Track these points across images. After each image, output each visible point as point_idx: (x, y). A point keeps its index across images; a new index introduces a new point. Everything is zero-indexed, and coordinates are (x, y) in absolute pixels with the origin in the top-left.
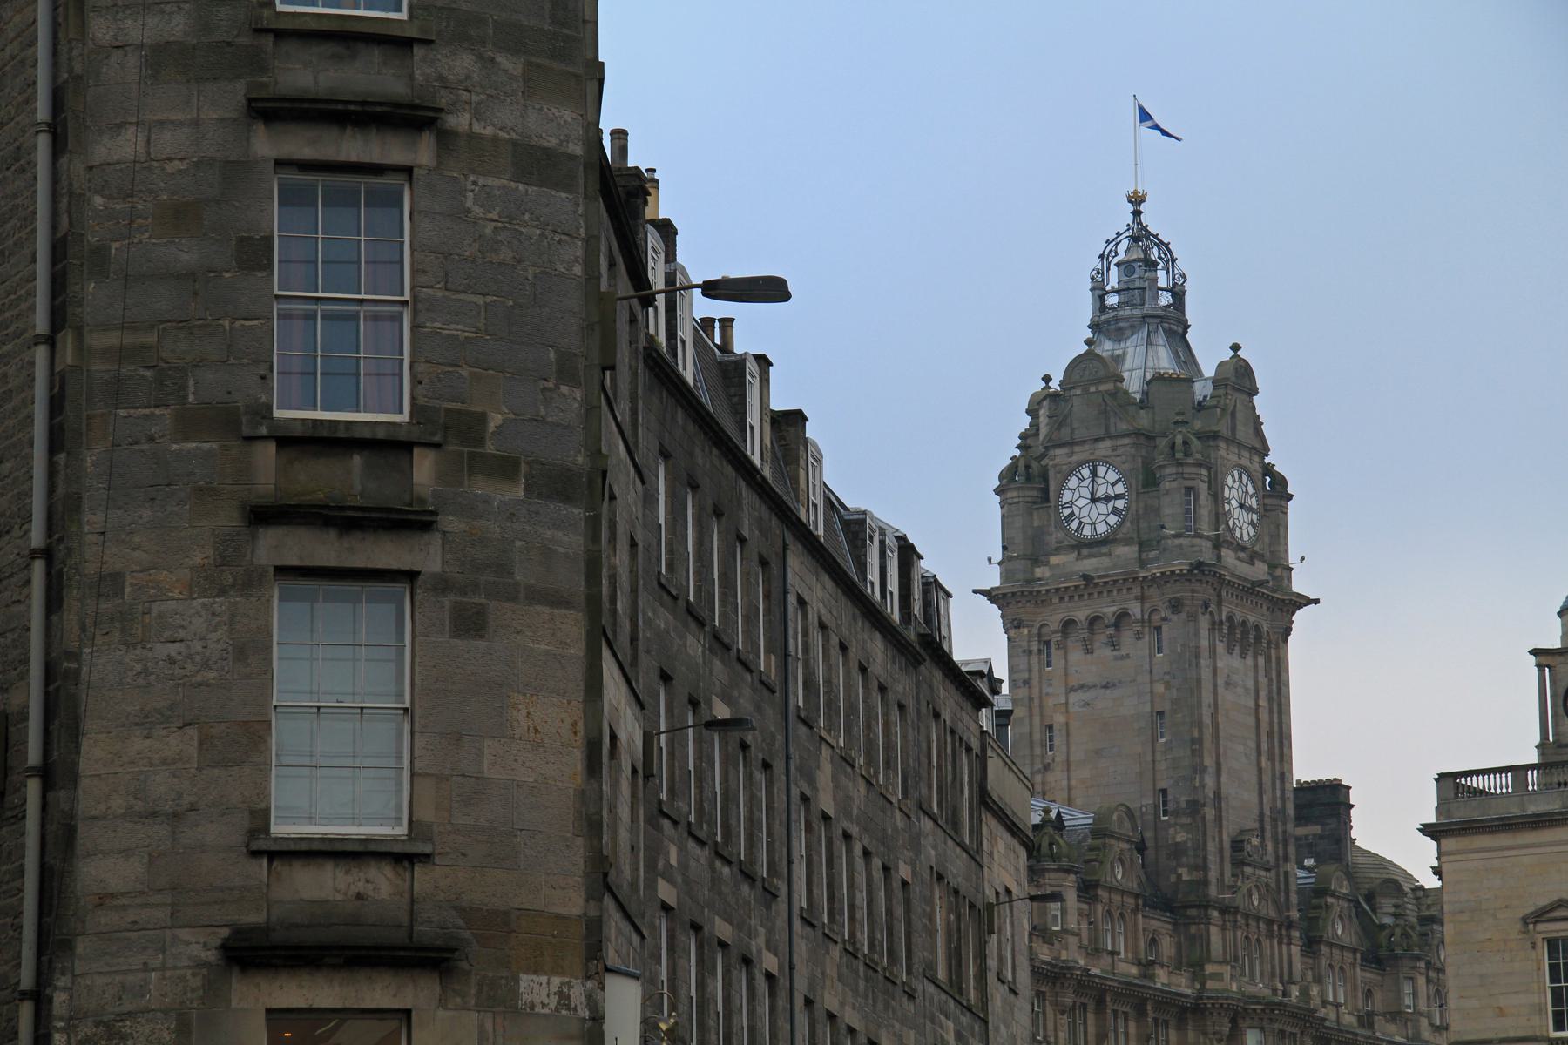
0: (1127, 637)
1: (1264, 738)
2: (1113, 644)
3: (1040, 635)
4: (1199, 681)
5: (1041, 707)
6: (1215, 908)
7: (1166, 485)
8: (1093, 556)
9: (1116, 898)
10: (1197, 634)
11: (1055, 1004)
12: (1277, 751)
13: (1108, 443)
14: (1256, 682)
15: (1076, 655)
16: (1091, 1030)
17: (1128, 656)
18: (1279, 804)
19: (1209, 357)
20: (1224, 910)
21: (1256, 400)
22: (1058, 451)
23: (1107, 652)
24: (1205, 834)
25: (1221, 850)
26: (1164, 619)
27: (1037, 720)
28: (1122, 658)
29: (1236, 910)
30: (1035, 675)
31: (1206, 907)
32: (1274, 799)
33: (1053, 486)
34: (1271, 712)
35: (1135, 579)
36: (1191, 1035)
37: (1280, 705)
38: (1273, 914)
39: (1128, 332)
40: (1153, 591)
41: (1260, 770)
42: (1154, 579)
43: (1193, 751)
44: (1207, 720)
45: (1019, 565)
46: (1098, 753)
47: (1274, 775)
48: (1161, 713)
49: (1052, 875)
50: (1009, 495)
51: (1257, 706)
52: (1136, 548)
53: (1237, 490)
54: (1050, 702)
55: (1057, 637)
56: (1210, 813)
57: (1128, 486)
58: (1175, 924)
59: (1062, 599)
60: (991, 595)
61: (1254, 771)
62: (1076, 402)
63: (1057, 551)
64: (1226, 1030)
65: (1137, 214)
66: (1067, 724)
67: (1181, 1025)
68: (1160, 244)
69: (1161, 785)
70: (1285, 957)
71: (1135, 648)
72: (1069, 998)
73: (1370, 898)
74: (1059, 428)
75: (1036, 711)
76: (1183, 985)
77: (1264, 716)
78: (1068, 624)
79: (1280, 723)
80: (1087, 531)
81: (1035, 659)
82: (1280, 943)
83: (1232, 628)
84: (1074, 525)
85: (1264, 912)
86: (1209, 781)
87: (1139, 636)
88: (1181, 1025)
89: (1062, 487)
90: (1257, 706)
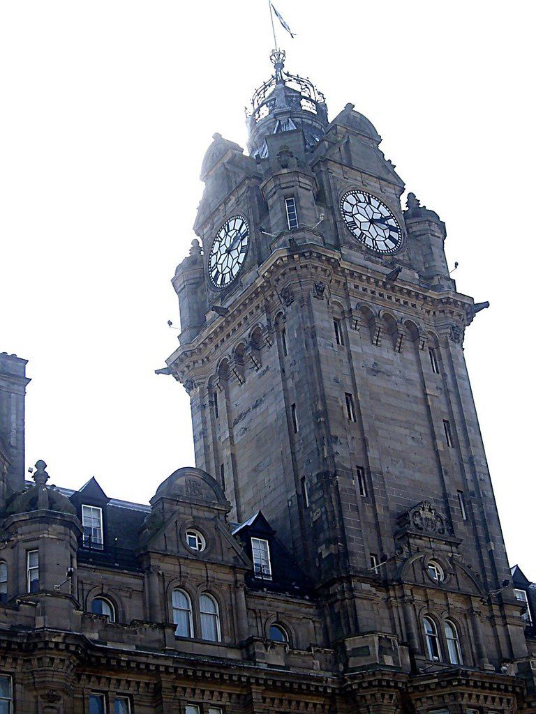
0: (265, 353)
2: (257, 365)
3: (210, 387)
4: (318, 356)
5: (216, 450)
7: (270, 202)
10: (311, 317)
12: (461, 438)
14: (421, 374)
18: (471, 487)
21: (381, 147)
23: (255, 374)
28: (264, 372)
30: (209, 424)
34: (449, 403)
43: (318, 425)
48: (294, 406)
49: (25, 529)
61: (432, 454)
65: (279, 66)
66: (233, 455)
68: (299, 81)
70: (503, 640)
76: (316, 667)
77: (439, 405)
80: (227, 280)
84: (219, 282)
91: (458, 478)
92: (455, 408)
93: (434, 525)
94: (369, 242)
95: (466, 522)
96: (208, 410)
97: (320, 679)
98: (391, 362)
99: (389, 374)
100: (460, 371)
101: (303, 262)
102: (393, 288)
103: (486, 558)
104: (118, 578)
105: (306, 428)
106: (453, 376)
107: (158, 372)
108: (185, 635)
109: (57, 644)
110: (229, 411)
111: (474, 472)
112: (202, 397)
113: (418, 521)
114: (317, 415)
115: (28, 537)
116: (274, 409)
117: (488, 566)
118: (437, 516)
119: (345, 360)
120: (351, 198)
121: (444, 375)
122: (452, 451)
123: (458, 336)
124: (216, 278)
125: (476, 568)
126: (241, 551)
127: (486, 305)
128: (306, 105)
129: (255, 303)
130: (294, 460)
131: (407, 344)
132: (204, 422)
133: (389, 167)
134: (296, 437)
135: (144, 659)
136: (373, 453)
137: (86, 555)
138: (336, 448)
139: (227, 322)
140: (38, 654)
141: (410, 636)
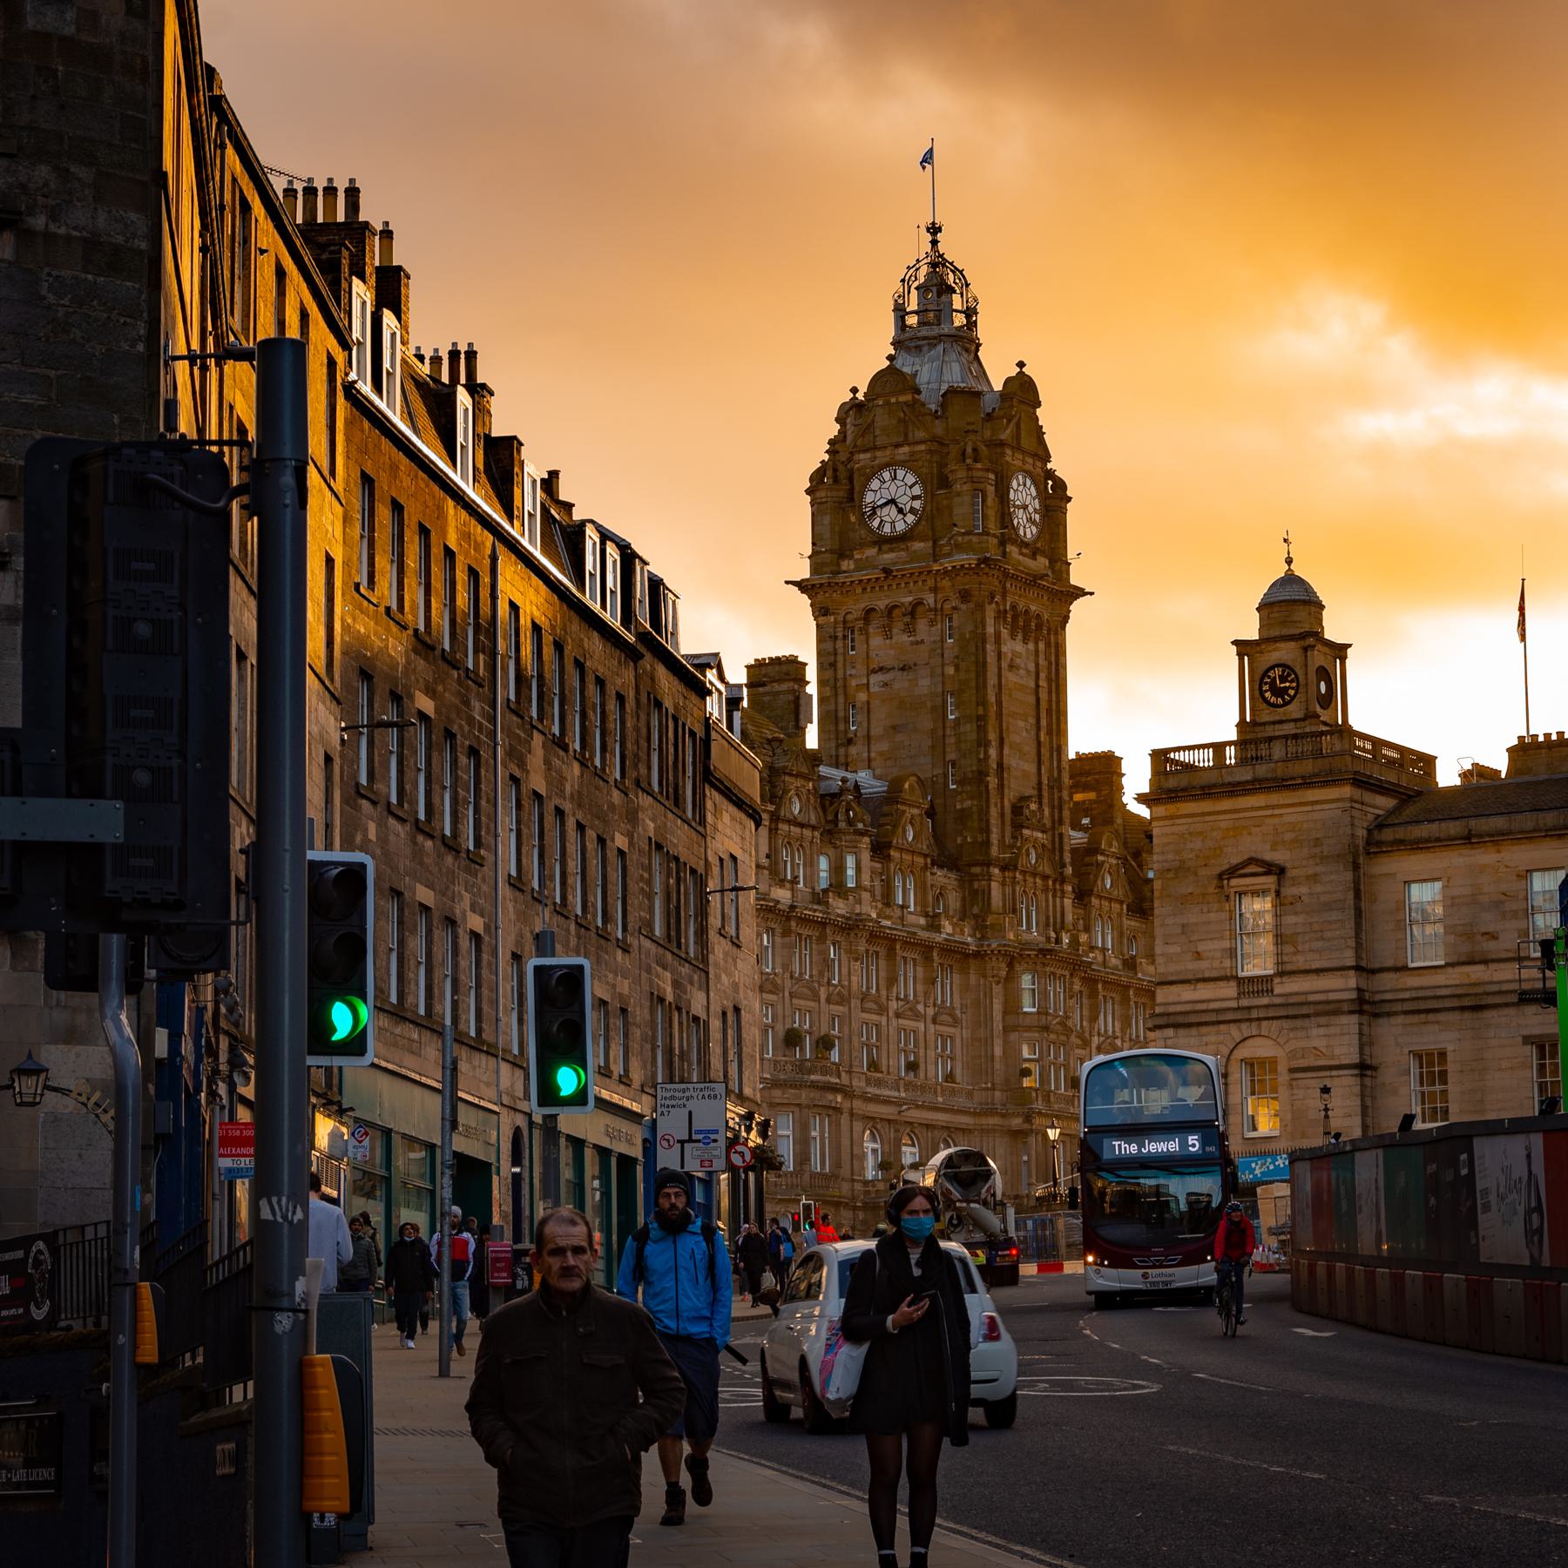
0: (922, 625)
1: (1043, 715)
2: (910, 629)
3: (845, 622)
8: (892, 550)
9: (907, 857)
11: (849, 951)
13: (906, 449)
14: (1037, 665)
15: (876, 641)
16: (882, 974)
17: (923, 641)
19: (998, 374)
21: (1039, 411)
22: (862, 456)
23: (905, 638)
24: (988, 800)
25: (1002, 815)
26: (954, 608)
27: (841, 699)
31: (988, 865)
32: (1051, 770)
33: (857, 488)
34: (1050, 692)
36: (973, 979)
39: (925, 349)
40: (946, 583)
41: (1039, 743)
42: (946, 572)
43: (979, 727)
44: (992, 699)
45: (828, 557)
46: (895, 728)
50: (818, 494)
51: (1038, 686)
52: (930, 544)
53: (1023, 493)
54: (854, 683)
55: (860, 624)
56: (993, 781)
57: (925, 489)
59: (864, 589)
60: (802, 586)
61: (1034, 745)
62: (879, 411)
63: (862, 545)
65: (934, 243)
67: (964, 972)
68: (955, 270)
72: (862, 947)
74: (863, 436)
75: (840, 691)
77: (1044, 695)
78: (869, 612)
80: (887, 529)
81: (839, 644)
82: (1054, 896)
83: (1015, 617)
84: (876, 523)
86: (993, 752)
87: (932, 623)
89: (865, 487)
90: (1038, 686)
96: (839, 644)
123: (1066, 619)
133: (1039, 433)
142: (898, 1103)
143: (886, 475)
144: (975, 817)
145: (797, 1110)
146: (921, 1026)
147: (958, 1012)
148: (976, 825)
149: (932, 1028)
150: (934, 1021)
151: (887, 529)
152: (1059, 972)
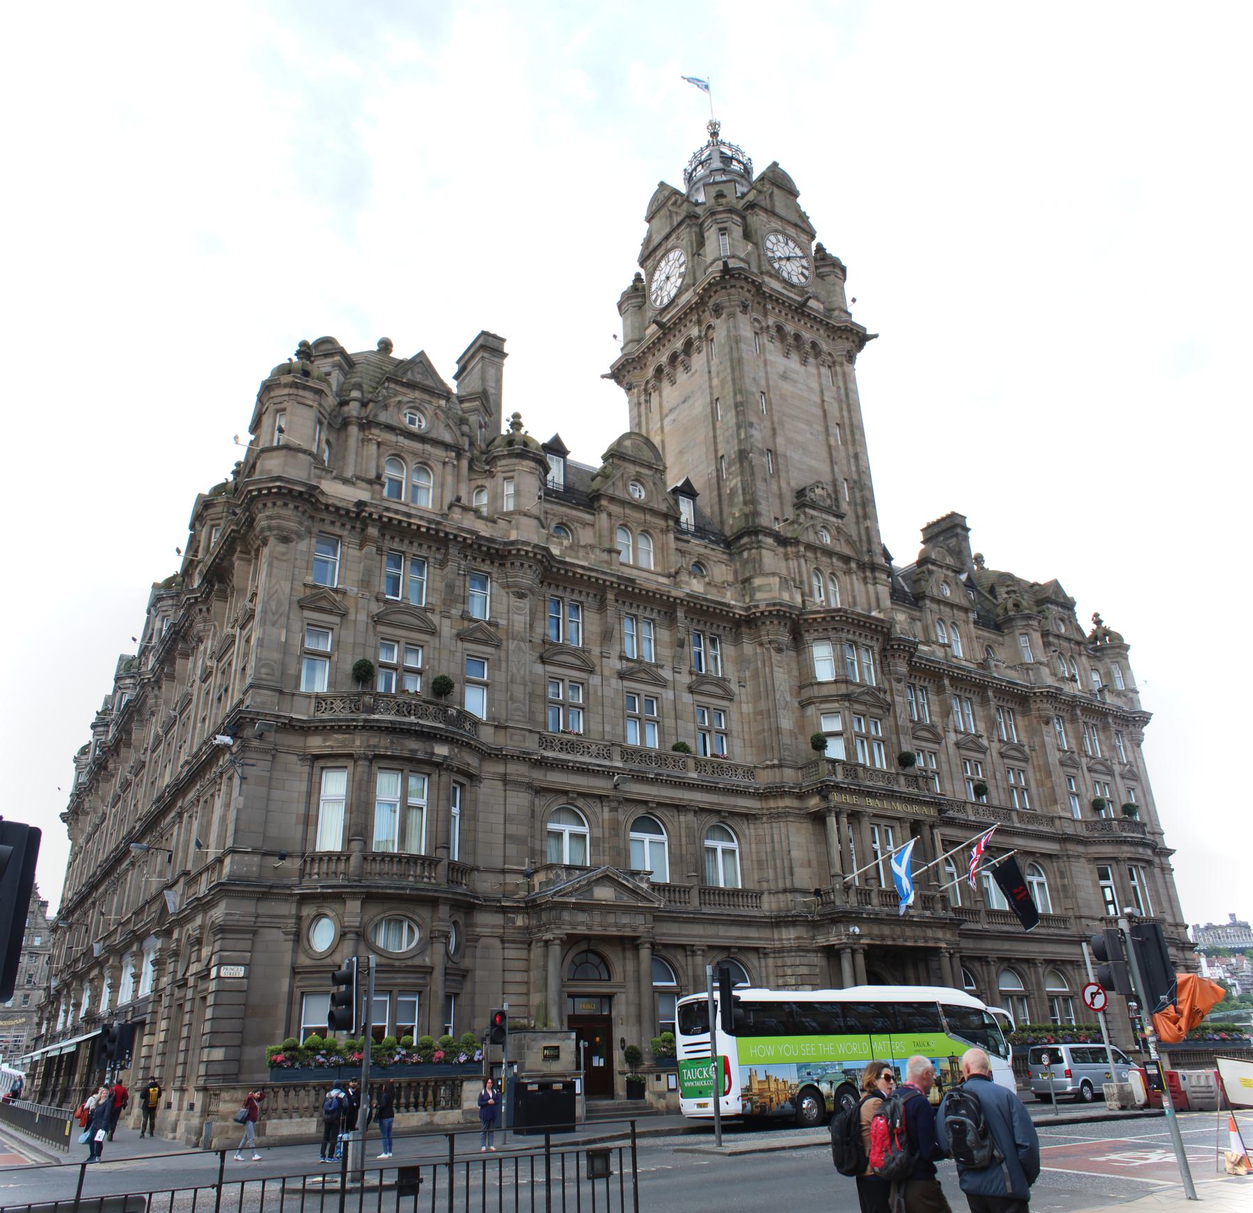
2: (687, 369)
3: (645, 390)
6: (767, 535)
7: (706, 235)
9: (638, 516)
11: (506, 586)
12: (849, 438)
13: (674, 236)
14: (821, 385)
18: (855, 477)
20: (783, 541)
21: (798, 200)
23: (685, 376)
24: (753, 474)
25: (781, 496)
29: (796, 542)
34: (841, 410)
35: (691, 309)
37: (849, 406)
38: (847, 551)
43: (737, 413)
47: (848, 456)
49: (503, 462)
55: (652, 382)
58: (730, 554)
61: (826, 448)
64: (785, 638)
65: (714, 134)
67: (737, 641)
68: (730, 146)
69: (720, 454)
71: (698, 361)
72: (526, 577)
73: (992, 590)
76: (729, 597)
77: (833, 409)
78: (659, 370)
79: (850, 418)
81: (643, 407)
85: (838, 549)
88: (737, 641)
91: (845, 469)
92: (845, 414)
93: (824, 501)
94: (785, 275)
95: (849, 503)
96: (643, 407)
97: (728, 605)
98: (797, 373)
99: (794, 381)
100: (850, 385)
101: (733, 282)
102: (803, 313)
103: (863, 532)
104: (575, 513)
105: (727, 418)
106: (846, 389)
107: (603, 377)
108: (625, 561)
109: (527, 552)
110: (661, 406)
111: (857, 465)
112: (639, 397)
113: (812, 495)
114: (736, 406)
115: (506, 469)
116: (700, 404)
117: (864, 538)
118: (829, 495)
119: (762, 365)
120: (772, 238)
121: (839, 388)
122: (842, 448)
123: (851, 359)
124: (655, 300)
125: (855, 538)
126: (672, 502)
127: (876, 336)
128: (735, 166)
129: (689, 317)
130: (715, 443)
131: (811, 360)
132: (640, 416)
133: (803, 217)
134: (718, 424)
135: (593, 574)
136: (780, 440)
137: (549, 494)
138: (754, 432)
139: (664, 334)
140: (511, 560)
141: (801, 582)
142: (608, 773)
143: (663, 264)
144: (740, 491)
145: (350, 764)
146: (668, 695)
147: (734, 687)
148: (741, 498)
149: (687, 698)
150: (691, 690)
151: (666, 301)
152: (862, 640)
